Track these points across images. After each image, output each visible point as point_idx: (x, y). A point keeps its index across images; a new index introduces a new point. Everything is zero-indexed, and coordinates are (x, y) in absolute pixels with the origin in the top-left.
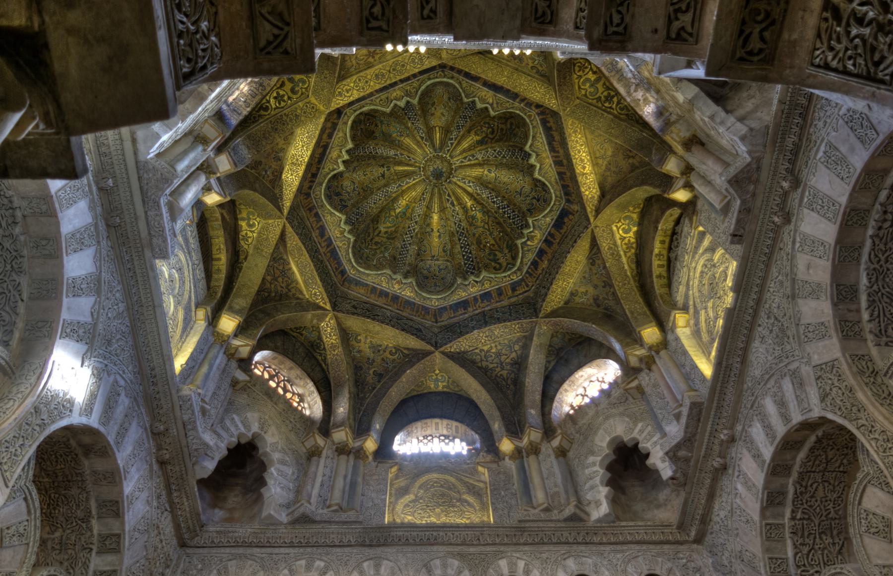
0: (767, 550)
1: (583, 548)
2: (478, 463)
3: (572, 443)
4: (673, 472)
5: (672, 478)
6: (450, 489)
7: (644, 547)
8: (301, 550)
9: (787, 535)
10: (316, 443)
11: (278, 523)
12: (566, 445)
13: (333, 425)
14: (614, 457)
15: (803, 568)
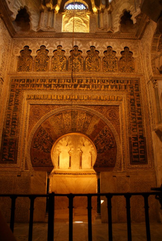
0: (152, 44)
1: (110, 39)
2: (87, 14)
3: (113, 10)
4: (137, 22)
5: (136, 24)
6: (79, 21)
7: (126, 40)
8: (41, 38)
9: (158, 41)
10: (42, 8)
11: (35, 32)
12: (111, 10)
13: (46, 2)
14: (123, 15)
15: (159, 49)
